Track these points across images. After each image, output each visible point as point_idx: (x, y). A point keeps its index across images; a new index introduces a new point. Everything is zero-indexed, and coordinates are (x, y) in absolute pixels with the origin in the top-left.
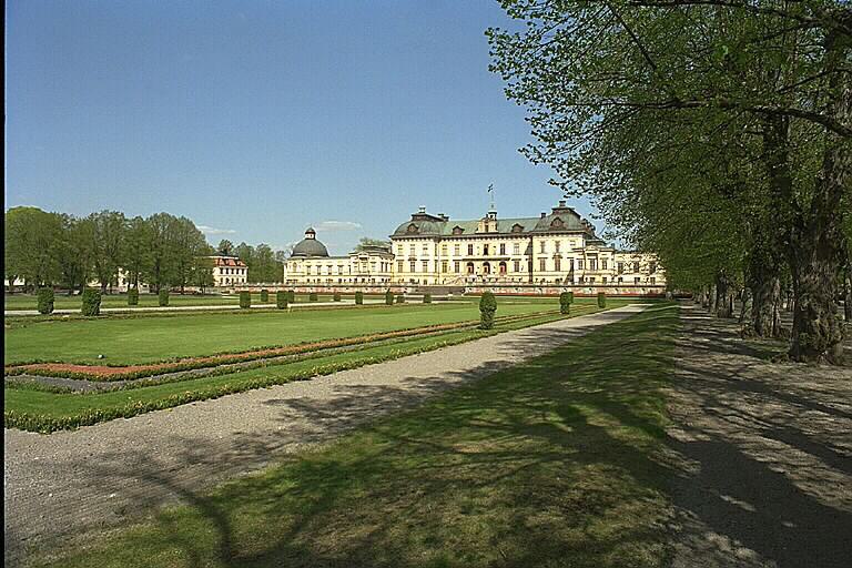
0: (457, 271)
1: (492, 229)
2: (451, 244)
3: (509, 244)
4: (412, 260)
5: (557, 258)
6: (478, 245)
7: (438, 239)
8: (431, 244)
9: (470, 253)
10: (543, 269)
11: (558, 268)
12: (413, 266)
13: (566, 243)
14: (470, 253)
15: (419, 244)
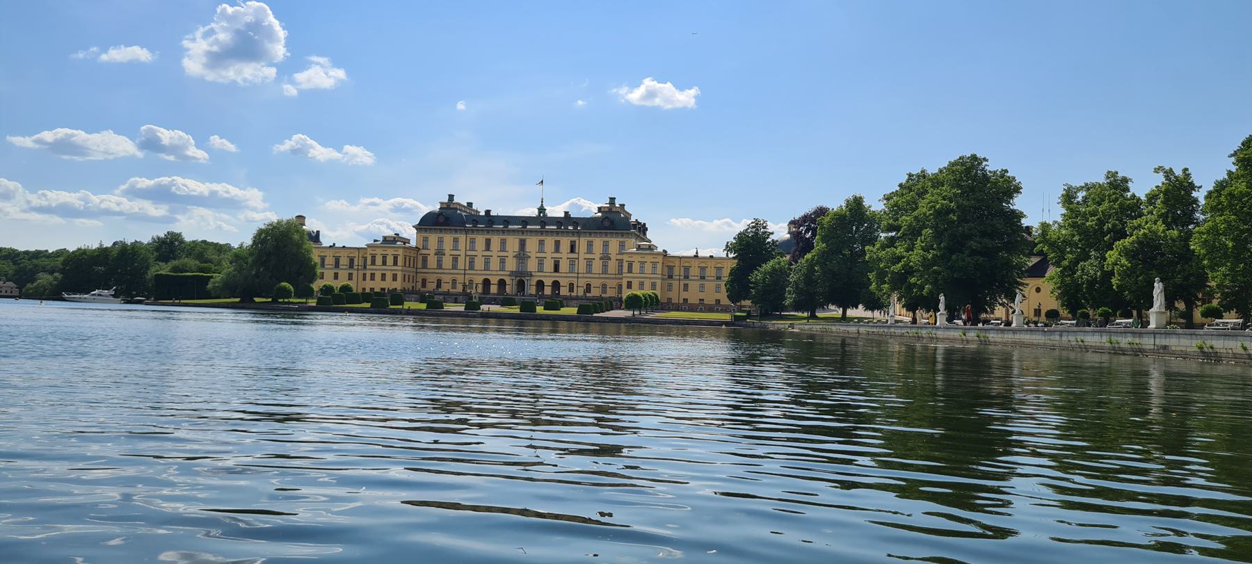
5: (605, 258)
10: (589, 270)
11: (605, 270)
15: (448, 238)
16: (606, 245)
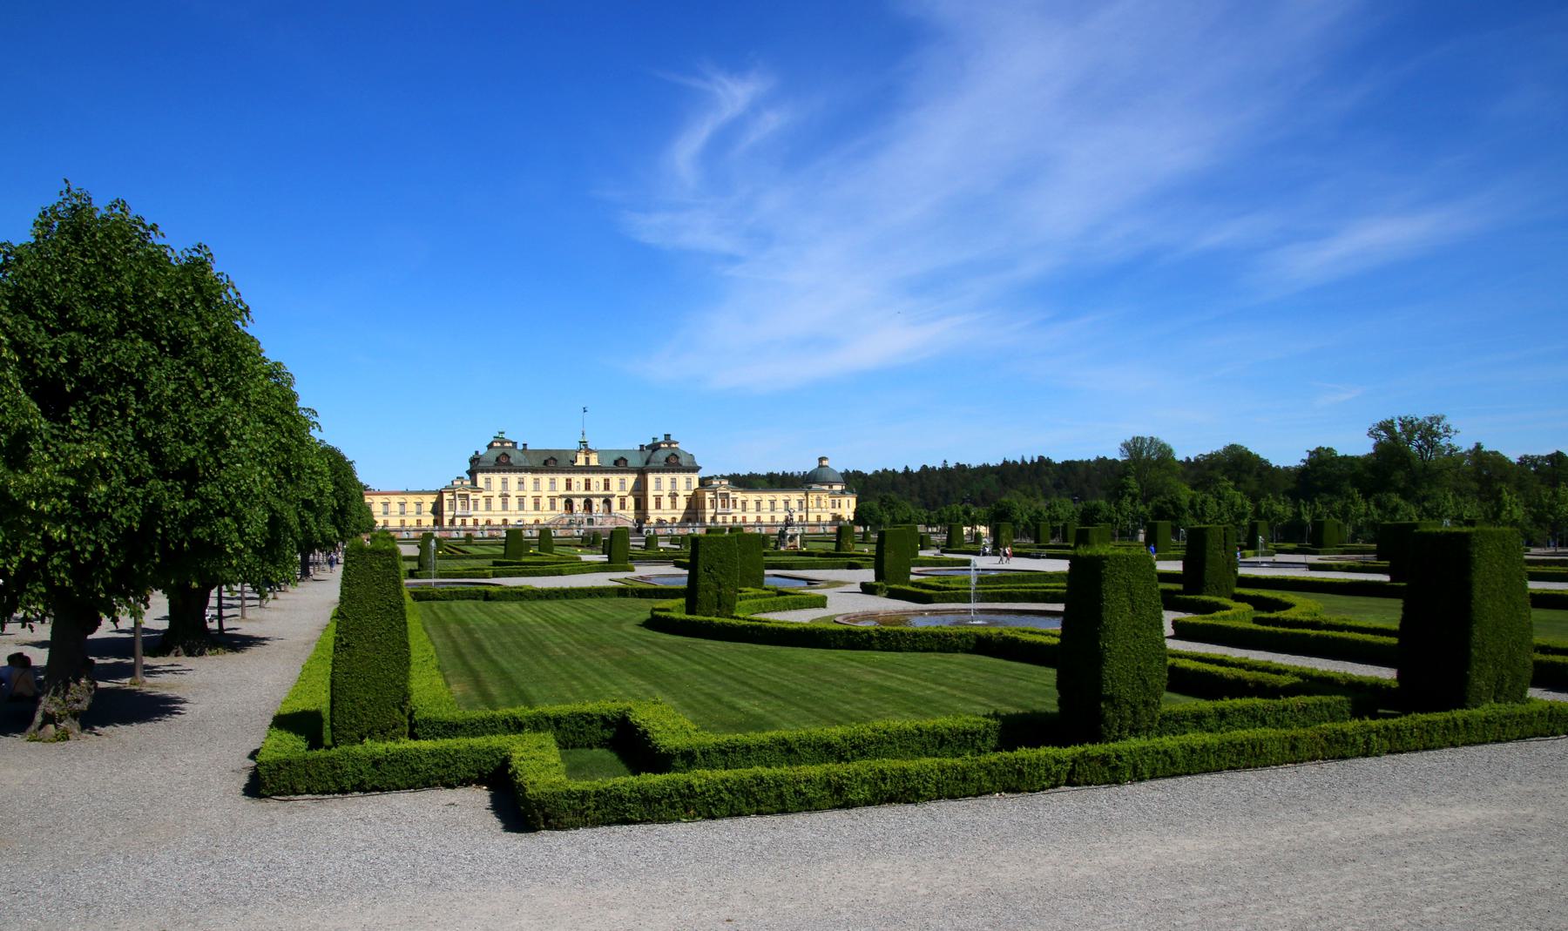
0: (553, 507)
1: (594, 461)
2: (545, 478)
3: (615, 479)
4: (505, 497)
5: (674, 496)
6: (578, 480)
7: (534, 471)
8: (529, 478)
9: (569, 486)
10: (658, 505)
11: (674, 504)
12: (505, 503)
13: (681, 478)
14: (569, 486)
15: (513, 478)
16: (674, 481)
